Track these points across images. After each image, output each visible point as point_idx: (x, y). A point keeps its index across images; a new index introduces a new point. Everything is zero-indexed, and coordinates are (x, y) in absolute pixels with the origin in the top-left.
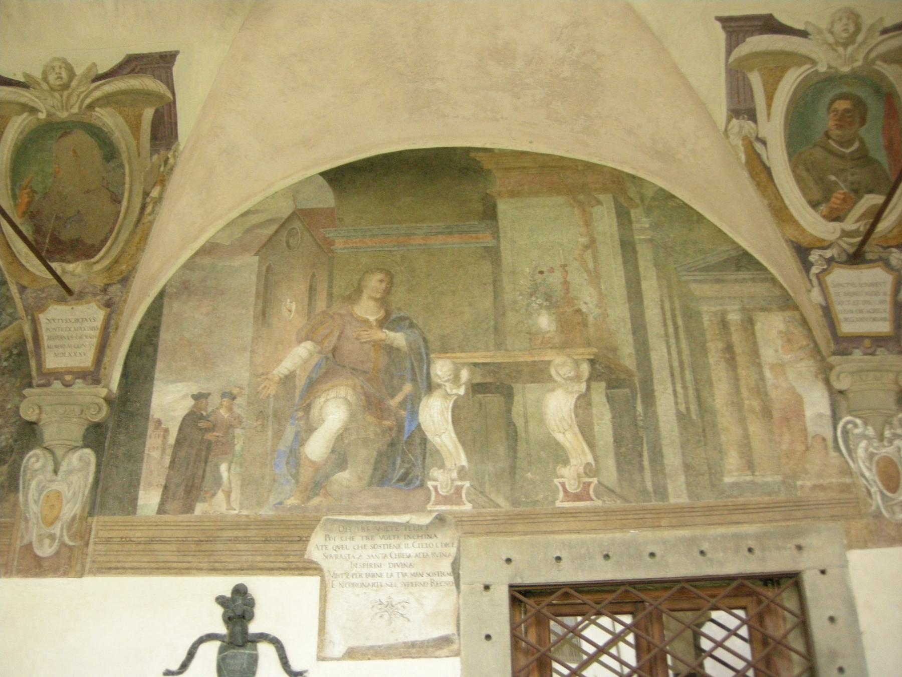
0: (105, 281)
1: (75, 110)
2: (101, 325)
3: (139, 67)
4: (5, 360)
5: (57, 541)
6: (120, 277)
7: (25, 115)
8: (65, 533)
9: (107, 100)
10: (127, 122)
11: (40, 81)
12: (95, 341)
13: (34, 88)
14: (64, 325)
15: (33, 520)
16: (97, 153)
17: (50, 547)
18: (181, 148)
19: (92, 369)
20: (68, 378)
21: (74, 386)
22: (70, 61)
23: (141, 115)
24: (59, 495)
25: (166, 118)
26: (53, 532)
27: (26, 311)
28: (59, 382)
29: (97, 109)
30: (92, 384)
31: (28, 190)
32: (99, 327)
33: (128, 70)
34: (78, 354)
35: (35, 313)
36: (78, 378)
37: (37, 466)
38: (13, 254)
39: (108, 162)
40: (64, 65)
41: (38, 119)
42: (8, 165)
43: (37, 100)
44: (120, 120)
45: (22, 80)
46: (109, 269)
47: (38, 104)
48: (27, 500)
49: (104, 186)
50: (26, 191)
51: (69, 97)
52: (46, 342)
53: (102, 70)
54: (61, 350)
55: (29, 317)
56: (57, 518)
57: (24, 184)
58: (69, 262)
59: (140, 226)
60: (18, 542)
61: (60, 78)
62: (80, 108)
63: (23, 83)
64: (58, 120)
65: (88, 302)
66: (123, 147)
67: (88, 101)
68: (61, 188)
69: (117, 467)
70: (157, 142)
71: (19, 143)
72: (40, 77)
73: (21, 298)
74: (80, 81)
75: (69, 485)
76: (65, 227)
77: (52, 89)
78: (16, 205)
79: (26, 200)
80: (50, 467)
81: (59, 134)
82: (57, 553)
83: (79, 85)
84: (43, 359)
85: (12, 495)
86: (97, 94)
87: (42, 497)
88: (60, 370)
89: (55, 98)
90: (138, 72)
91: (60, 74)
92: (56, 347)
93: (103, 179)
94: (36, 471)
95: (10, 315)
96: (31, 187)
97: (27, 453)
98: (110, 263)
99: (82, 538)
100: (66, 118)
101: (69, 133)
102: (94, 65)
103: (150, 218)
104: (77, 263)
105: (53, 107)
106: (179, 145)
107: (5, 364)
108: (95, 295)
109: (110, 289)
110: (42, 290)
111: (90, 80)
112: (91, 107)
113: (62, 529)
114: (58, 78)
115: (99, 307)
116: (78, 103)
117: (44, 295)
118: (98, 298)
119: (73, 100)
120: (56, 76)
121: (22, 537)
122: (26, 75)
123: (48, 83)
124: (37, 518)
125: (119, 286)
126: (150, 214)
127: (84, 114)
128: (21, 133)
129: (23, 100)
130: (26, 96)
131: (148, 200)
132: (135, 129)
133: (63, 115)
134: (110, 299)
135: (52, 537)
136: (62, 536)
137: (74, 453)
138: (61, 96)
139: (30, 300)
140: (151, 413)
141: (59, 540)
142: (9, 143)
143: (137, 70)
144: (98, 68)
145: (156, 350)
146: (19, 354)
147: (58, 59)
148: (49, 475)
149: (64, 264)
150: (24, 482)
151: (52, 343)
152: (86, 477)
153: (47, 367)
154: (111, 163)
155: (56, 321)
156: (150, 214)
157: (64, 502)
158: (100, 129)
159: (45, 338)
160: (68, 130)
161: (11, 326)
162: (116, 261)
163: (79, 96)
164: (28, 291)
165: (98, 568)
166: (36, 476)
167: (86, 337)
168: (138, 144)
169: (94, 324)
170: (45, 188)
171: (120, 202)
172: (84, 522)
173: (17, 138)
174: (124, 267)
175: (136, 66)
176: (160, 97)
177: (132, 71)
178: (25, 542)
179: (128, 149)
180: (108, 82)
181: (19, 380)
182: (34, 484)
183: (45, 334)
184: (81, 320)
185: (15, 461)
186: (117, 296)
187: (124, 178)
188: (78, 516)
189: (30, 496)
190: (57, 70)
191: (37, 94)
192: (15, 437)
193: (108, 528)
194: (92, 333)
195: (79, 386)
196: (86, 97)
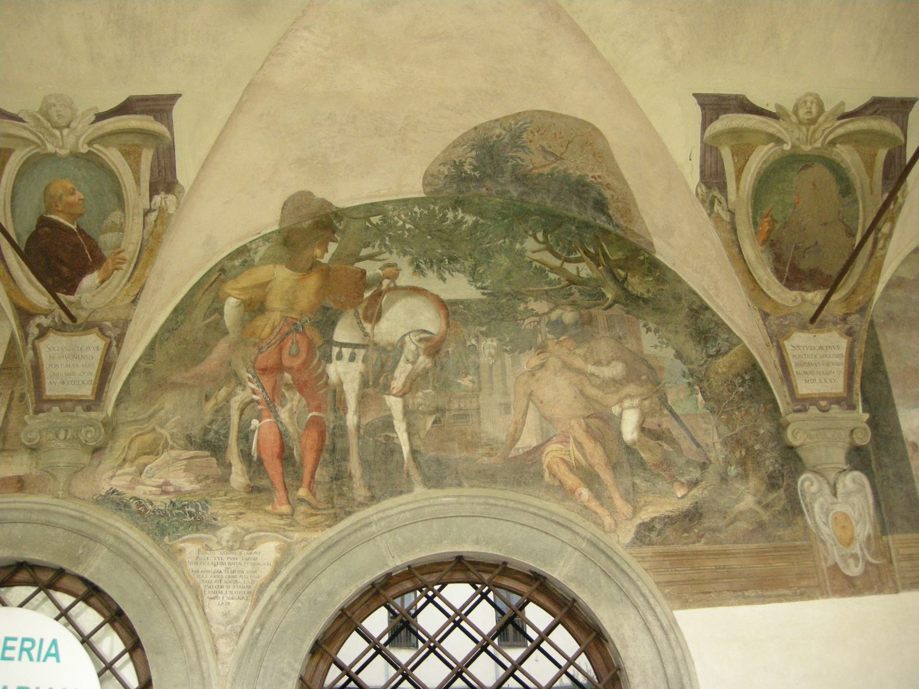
0: (844, 311)
1: (818, 144)
2: (846, 352)
3: (881, 109)
4: (740, 386)
5: (861, 560)
6: (858, 308)
7: (771, 145)
8: (866, 553)
9: (847, 138)
10: (862, 159)
11: (790, 113)
12: (842, 368)
13: (784, 120)
14: (810, 352)
15: (830, 542)
16: (834, 188)
17: (857, 566)
18: (909, 189)
19: (845, 395)
20: (823, 403)
21: (830, 412)
22: (822, 97)
23: (875, 155)
24: (846, 517)
25: (896, 160)
26: (853, 552)
27: (770, 337)
28: (814, 407)
29: (838, 145)
30: (847, 410)
31: (768, 219)
32: (844, 354)
33: (871, 111)
34: (828, 380)
35: (781, 341)
36: (834, 404)
37: (814, 488)
38: (754, 280)
39: (844, 197)
40: (815, 101)
41: (783, 150)
42: (750, 193)
43: (785, 132)
44: (857, 157)
45: (774, 111)
46: (846, 299)
47: (785, 136)
48: (815, 523)
49: (840, 220)
50: (766, 219)
51: (814, 132)
52: (794, 369)
53: (849, 109)
54: (811, 377)
55: (775, 344)
56: (852, 539)
57: (765, 211)
58: (808, 291)
59: (874, 260)
60: (823, 563)
61: (810, 112)
62: (823, 143)
63: (774, 114)
64: (801, 152)
65: (830, 331)
66: (857, 184)
67: (831, 137)
68: (800, 219)
69: (892, 487)
70: (888, 182)
71: (762, 172)
72: (791, 110)
73: (765, 325)
74: (827, 118)
75: (853, 505)
76: (804, 257)
77: (800, 123)
78: (756, 233)
79: (767, 228)
80: (827, 490)
81: (801, 166)
82: (866, 572)
83: (825, 121)
84: (794, 384)
85: (799, 518)
86: (841, 131)
87: (830, 519)
88: (814, 396)
89: (801, 131)
90: (879, 115)
91: (811, 108)
92: (806, 373)
93: (839, 212)
94: (814, 494)
95: (727, 340)
96: (772, 216)
97: (799, 477)
98: (848, 293)
99: (884, 556)
100: (810, 151)
101: (810, 166)
102: (843, 104)
103: (882, 252)
104: (816, 292)
105: (798, 139)
106: (907, 186)
107: (741, 389)
108: (835, 323)
109: (851, 319)
110: (785, 317)
111: (836, 117)
112: (833, 143)
113: (861, 549)
114: (808, 112)
115: (841, 336)
116: (821, 139)
117: (786, 323)
118: (839, 326)
119: (818, 135)
120: (806, 110)
121: (826, 559)
122: (778, 107)
123: (797, 116)
124: (833, 540)
125: (858, 316)
126: (882, 249)
127: (827, 149)
128: (765, 162)
129: (771, 130)
130: (775, 127)
131: (880, 235)
132: (870, 167)
133: (807, 148)
134: (851, 328)
135: (855, 557)
136: (864, 556)
137: (845, 475)
138: (808, 130)
139: (774, 327)
140: (905, 436)
141: (863, 559)
142: (752, 171)
143: (878, 112)
144: (846, 107)
145: (886, 377)
146: (753, 380)
147: (811, 94)
148: (830, 498)
149: (803, 293)
150: (806, 506)
151: (800, 369)
152: (866, 497)
153: (800, 393)
154: (846, 198)
155: (802, 348)
156: (882, 249)
157: (854, 523)
158: (839, 164)
159: (793, 365)
160: (809, 164)
161: (732, 352)
162: (853, 292)
163: (823, 131)
164: (772, 318)
165: (911, 583)
166: (816, 499)
167: (833, 364)
168: (871, 181)
169: (839, 352)
170: (785, 218)
171: (854, 236)
172: (881, 542)
173: (761, 167)
174: (861, 298)
175: (878, 109)
176: (895, 139)
177: (874, 113)
178: (830, 563)
179: (862, 188)
180: (852, 121)
181: (762, 405)
182: (816, 507)
183: (792, 361)
184: (825, 348)
185: (789, 485)
186: (857, 325)
187: (858, 213)
188: (872, 536)
189: (817, 518)
190: (809, 104)
191: (785, 126)
192: (780, 461)
193: (906, 545)
194: (838, 360)
195: (835, 410)
196: (830, 133)
